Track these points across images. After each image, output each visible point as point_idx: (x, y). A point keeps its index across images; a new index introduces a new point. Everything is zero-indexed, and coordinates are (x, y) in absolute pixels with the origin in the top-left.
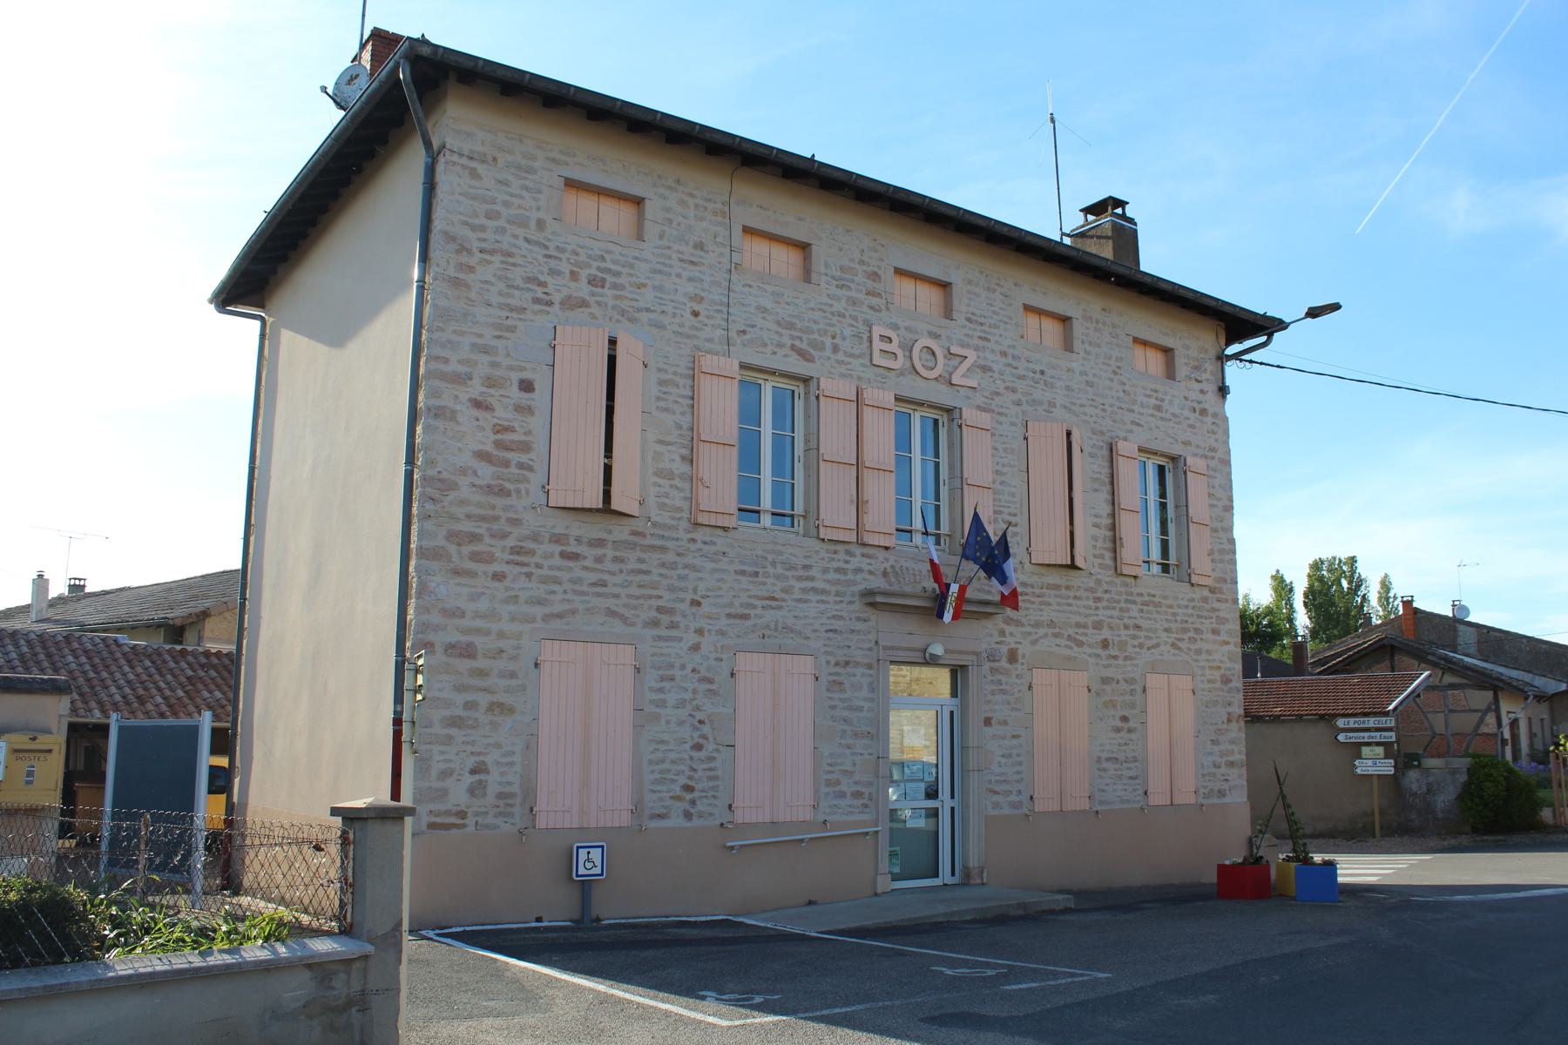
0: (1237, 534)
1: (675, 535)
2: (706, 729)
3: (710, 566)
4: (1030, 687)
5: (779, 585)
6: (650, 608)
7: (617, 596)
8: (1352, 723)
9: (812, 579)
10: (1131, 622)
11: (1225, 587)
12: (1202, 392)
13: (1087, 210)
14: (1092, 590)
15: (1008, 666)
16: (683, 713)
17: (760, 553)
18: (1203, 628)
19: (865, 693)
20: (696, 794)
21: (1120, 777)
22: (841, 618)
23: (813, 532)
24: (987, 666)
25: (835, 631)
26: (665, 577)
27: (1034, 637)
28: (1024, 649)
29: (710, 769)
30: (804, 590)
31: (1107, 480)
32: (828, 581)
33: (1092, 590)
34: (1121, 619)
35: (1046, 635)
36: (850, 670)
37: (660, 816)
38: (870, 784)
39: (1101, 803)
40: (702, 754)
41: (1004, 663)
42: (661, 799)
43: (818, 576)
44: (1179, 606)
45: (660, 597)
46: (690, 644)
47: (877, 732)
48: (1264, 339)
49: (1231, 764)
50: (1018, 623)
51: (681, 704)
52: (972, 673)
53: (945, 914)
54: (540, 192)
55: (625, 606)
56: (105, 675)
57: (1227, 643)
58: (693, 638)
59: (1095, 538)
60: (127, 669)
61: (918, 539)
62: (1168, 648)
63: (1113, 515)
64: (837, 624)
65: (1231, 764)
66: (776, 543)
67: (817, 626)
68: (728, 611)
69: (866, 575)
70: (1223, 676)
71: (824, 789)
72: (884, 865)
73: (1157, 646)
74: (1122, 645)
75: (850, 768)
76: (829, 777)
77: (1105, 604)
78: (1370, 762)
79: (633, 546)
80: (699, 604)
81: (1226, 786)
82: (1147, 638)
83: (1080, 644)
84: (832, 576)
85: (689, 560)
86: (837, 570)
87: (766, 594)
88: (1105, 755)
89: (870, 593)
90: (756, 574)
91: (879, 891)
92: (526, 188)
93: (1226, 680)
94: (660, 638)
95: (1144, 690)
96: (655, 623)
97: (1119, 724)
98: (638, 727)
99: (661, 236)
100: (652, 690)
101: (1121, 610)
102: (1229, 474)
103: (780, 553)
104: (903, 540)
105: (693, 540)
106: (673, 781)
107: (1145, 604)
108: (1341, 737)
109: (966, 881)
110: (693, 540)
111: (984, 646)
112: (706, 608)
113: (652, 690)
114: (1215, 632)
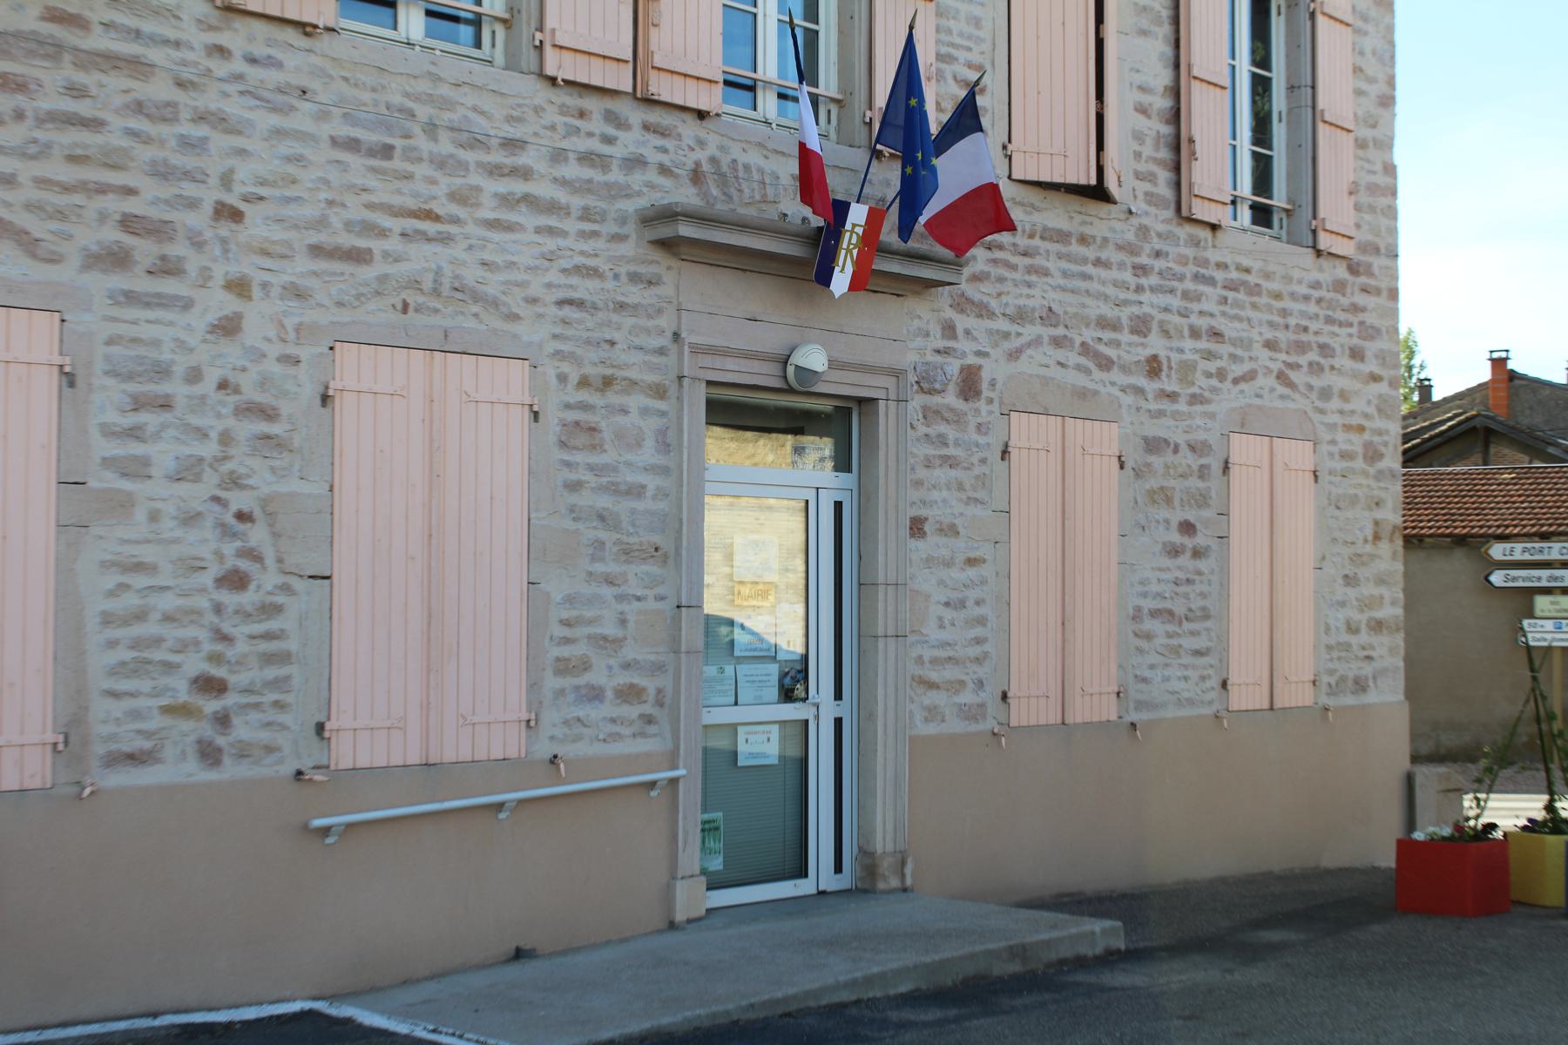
0: (1401, 155)
1: (172, 34)
2: (257, 535)
3: (267, 120)
4: (1005, 453)
5: (445, 183)
6: (103, 217)
8: (1518, 551)
9: (525, 174)
10: (1203, 323)
11: (1377, 263)
14: (1131, 250)
15: (960, 404)
16: (196, 494)
17: (397, 99)
18: (1334, 343)
19: (648, 454)
20: (230, 700)
21: (1176, 651)
22: (595, 273)
23: (529, 58)
24: (917, 402)
25: (579, 304)
26: (147, 140)
27: (1017, 343)
28: (994, 369)
29: (268, 636)
30: (506, 201)
31: (1166, 14)
32: (563, 182)
33: (1131, 250)
34: (1184, 314)
35: (1037, 342)
36: (613, 398)
37: (135, 758)
38: (658, 668)
39: (1140, 705)
40: (248, 598)
41: (951, 399)
42: (136, 715)
43: (541, 166)
44: (1293, 296)
45: (130, 192)
46: (212, 317)
47: (676, 548)
49: (1378, 626)
50: (983, 311)
51: (188, 471)
52: (886, 416)
53: (852, 984)
55: (30, 207)
57: (1375, 378)
58: (220, 303)
59: (1139, 137)
61: (768, 103)
62: (1271, 381)
63: (1175, 92)
64: (584, 288)
65: (1378, 626)
66: (436, 79)
67: (535, 289)
68: (314, 238)
69: (652, 176)
70: (1368, 445)
71: (552, 682)
72: (691, 857)
73: (1250, 376)
74: (1187, 369)
75: (611, 630)
76: (565, 651)
77: (1154, 280)
78: (1549, 625)
79: (54, 51)
80: (236, 216)
81: (1368, 670)
82: (1234, 358)
83: (1106, 364)
84: (572, 170)
85: (209, 100)
86: (586, 158)
87: (412, 204)
88: (1149, 604)
89: (669, 215)
90: (387, 151)
91: (680, 917)
93: (1373, 455)
94: (131, 298)
95: (1226, 468)
96: (118, 259)
97: (1176, 537)
98: (71, 528)
100: (108, 432)
101: (1186, 295)
102: (1390, 29)
103: (446, 104)
104: (733, 108)
105: (221, 51)
106: (169, 667)
107: (1231, 286)
108: (1497, 578)
109: (865, 888)
110: (221, 51)
111: (912, 358)
112: (257, 225)
113: (108, 432)
114: (1357, 354)
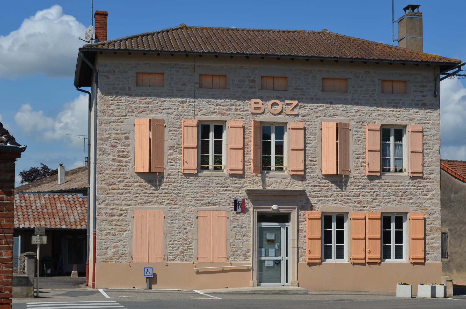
7: (158, 197)
12: (423, 96)
13: (405, 9)
48: (457, 69)
54: (129, 78)
56: (70, 211)
60: (79, 208)
83: (347, 203)
92: (123, 78)
99: (170, 85)
